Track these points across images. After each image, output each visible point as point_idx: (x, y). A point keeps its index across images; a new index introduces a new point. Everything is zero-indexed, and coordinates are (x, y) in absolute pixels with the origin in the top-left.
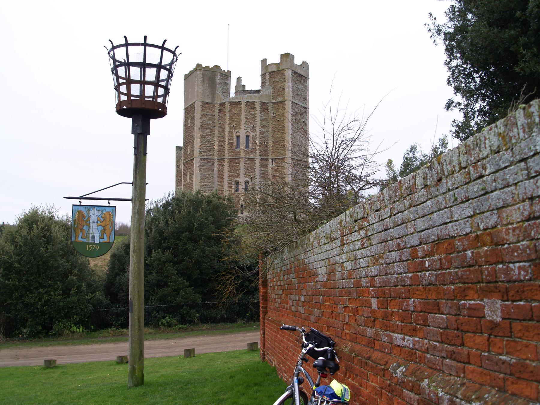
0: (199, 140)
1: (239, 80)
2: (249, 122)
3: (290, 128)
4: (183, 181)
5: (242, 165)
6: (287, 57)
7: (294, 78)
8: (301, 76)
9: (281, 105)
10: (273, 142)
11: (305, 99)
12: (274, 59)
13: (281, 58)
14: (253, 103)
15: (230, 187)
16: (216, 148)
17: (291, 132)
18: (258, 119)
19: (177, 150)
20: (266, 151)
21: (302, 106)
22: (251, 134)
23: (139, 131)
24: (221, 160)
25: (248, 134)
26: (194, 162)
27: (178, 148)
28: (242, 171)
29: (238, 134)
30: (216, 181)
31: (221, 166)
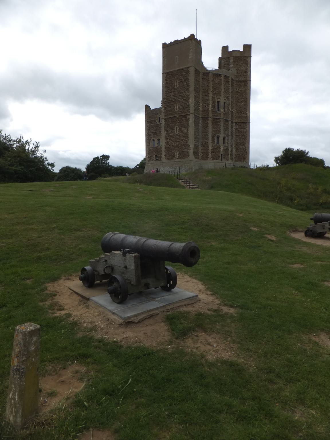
5: (222, 124)
9: (243, 84)
10: (236, 110)
15: (213, 140)
16: (201, 108)
25: (225, 101)
28: (222, 128)
29: (219, 100)
31: (205, 123)
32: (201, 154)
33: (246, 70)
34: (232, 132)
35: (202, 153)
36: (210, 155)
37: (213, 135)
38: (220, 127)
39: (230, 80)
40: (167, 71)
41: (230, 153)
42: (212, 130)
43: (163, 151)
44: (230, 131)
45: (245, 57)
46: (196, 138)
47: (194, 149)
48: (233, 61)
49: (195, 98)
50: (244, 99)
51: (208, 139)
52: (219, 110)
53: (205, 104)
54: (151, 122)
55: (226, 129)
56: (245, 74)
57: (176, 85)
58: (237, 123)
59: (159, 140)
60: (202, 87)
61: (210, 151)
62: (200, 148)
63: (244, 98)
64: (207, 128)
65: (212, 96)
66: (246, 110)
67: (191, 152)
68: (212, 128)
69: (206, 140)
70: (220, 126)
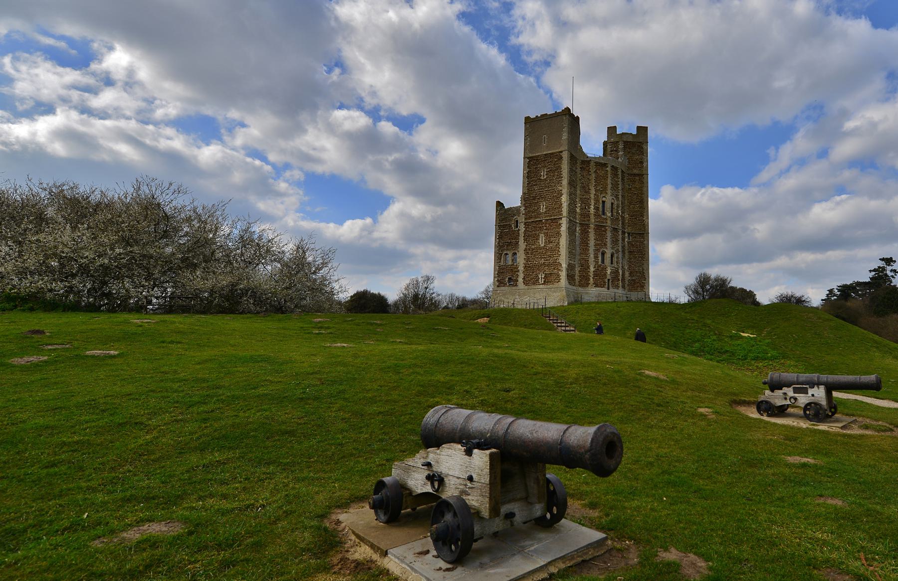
5: (609, 234)
9: (637, 178)
15: (596, 257)
16: (578, 210)
28: (609, 240)
34: (623, 247)
39: (620, 173)
41: (620, 278)
43: (521, 272)
44: (620, 244)
46: (571, 253)
47: (567, 270)
49: (570, 195)
52: (604, 213)
54: (504, 226)
55: (615, 242)
57: (543, 174)
59: (515, 254)
61: (591, 274)
62: (577, 269)
66: (642, 216)
67: (563, 274)
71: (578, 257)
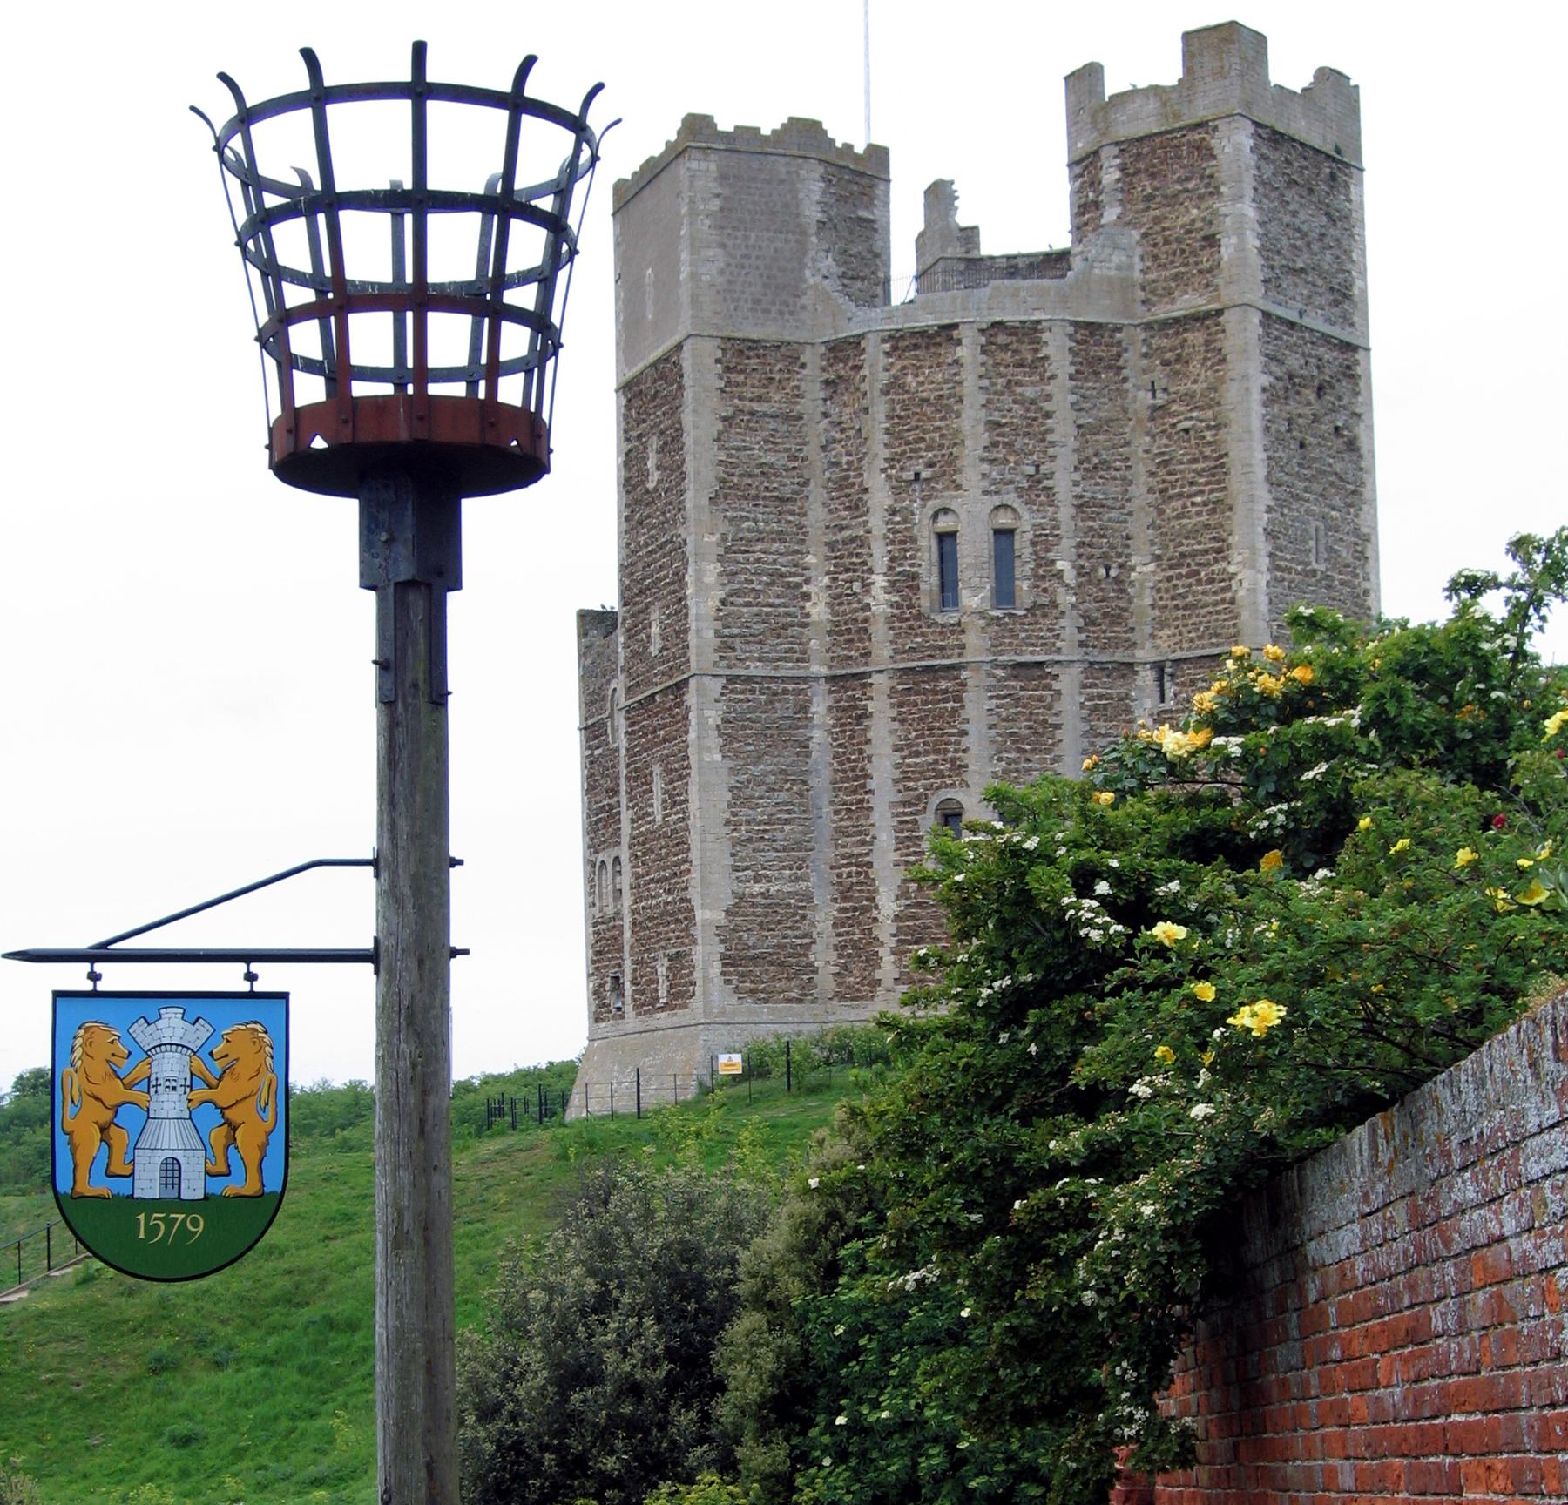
0: (712, 571)
1: (940, 196)
2: (1009, 445)
3: (1261, 471)
4: (626, 816)
5: (977, 709)
6: (1223, 49)
7: (1268, 170)
8: (1313, 158)
9: (1196, 337)
10: (1158, 558)
11: (1344, 295)
12: (1147, 62)
13: (1189, 55)
14: (1031, 331)
16: (818, 610)
17: (1264, 497)
18: (1063, 428)
19: (583, 633)
20: (1116, 618)
21: (1326, 338)
22: (1026, 523)
23: (405, 571)
24: (849, 684)
25: (1005, 520)
26: (691, 699)
27: (593, 623)
29: (944, 524)
30: (828, 810)
31: (852, 718)
32: (833, 956)
33: (1213, 229)
35: (840, 948)
36: (887, 958)
37: (905, 804)
38: (964, 733)
40: (630, 374)
42: (897, 766)
45: (1199, 125)
46: (746, 842)
48: (1117, 175)
50: (1206, 458)
51: (874, 838)
53: (847, 570)
56: (1204, 255)
58: (1168, 670)
60: (824, 448)
61: (886, 931)
62: (824, 916)
63: (1207, 451)
64: (861, 752)
65: (889, 502)
67: (706, 956)
68: (897, 749)
69: (856, 851)
70: (967, 721)
71: (825, 854)
